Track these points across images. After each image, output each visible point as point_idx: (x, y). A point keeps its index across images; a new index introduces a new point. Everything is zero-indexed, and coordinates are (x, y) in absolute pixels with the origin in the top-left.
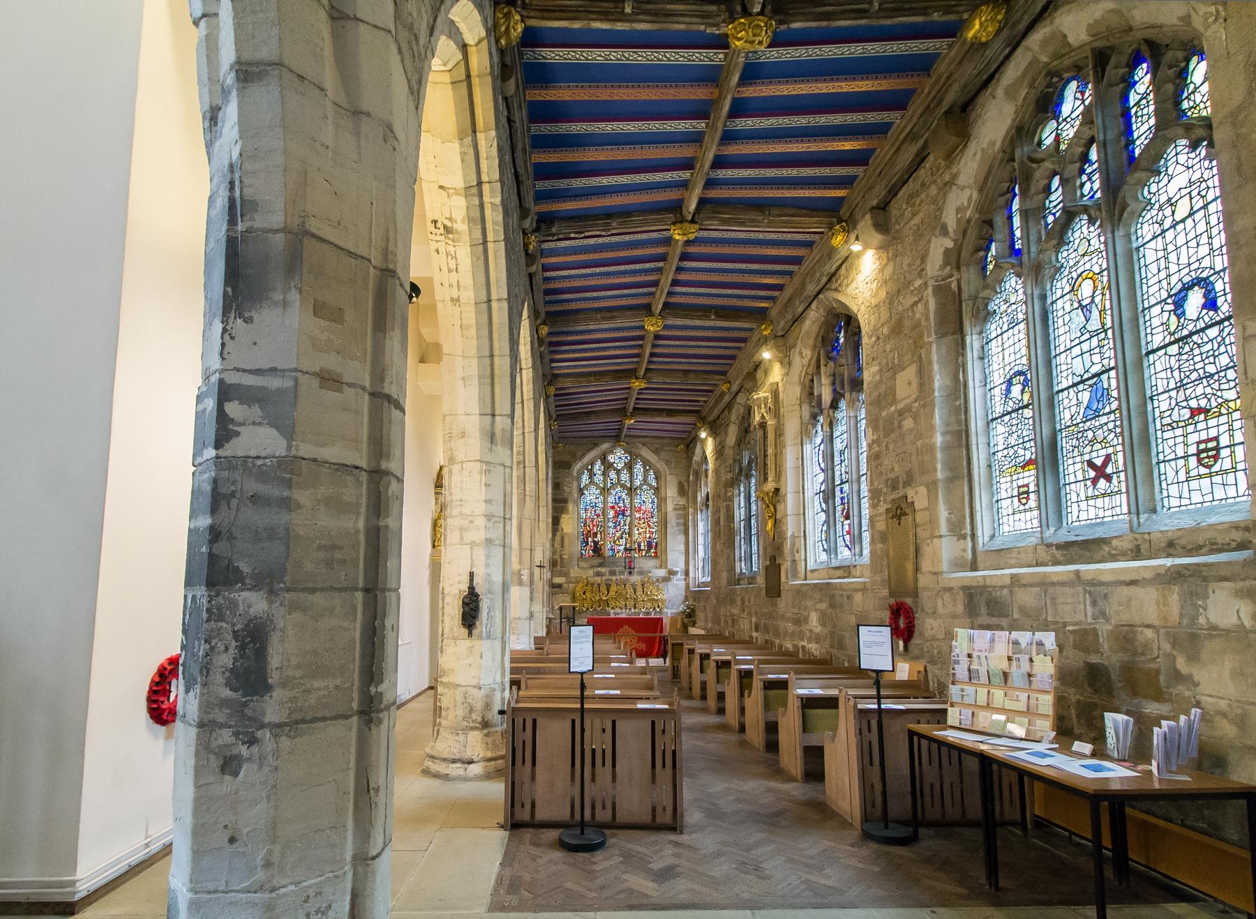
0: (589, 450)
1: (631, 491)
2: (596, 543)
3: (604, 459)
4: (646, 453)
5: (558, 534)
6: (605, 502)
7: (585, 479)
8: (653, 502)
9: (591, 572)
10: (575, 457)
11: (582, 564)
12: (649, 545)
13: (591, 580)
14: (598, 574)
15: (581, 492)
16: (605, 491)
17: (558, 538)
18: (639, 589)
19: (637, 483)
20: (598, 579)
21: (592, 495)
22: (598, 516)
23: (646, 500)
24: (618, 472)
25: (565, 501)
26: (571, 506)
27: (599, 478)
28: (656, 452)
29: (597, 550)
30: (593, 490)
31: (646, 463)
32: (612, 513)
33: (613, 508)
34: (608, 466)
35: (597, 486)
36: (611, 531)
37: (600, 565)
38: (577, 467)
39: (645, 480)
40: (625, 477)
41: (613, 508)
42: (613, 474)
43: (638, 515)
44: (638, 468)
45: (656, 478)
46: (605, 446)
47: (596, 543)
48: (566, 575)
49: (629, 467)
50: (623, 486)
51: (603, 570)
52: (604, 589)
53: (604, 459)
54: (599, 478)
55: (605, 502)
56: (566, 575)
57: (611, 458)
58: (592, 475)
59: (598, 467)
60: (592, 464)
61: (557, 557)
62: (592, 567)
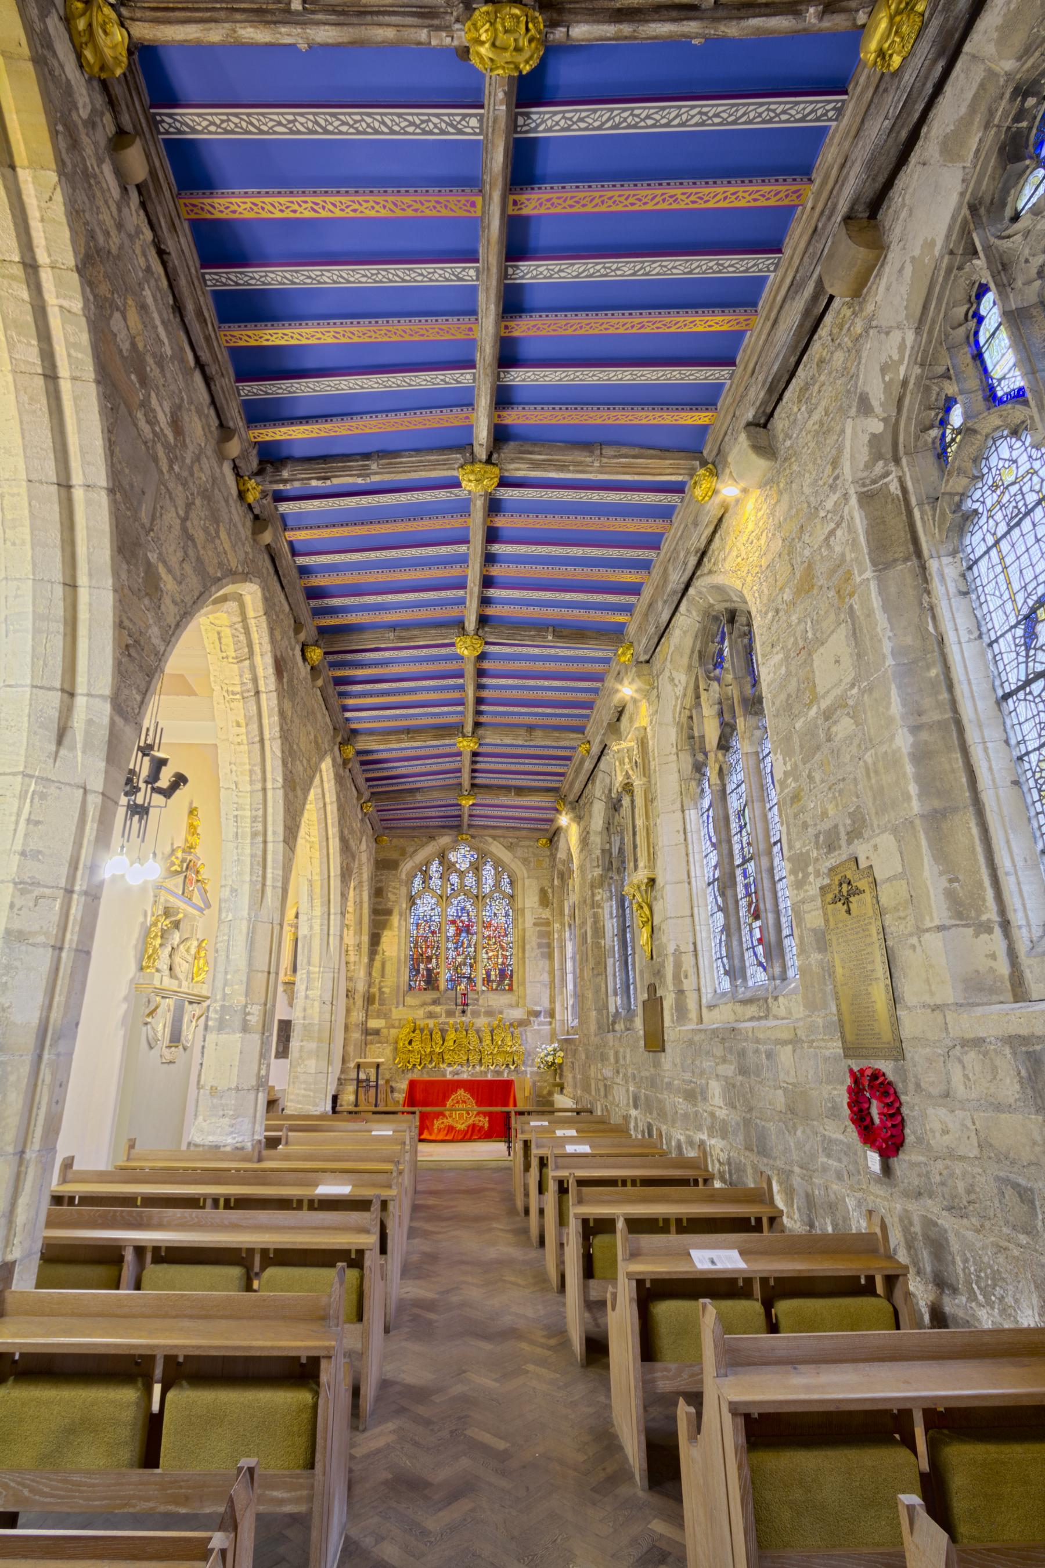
1: (478, 898)
2: (429, 971)
3: (442, 856)
4: (497, 849)
5: (378, 958)
7: (418, 881)
8: (507, 915)
9: (420, 1013)
11: (409, 1000)
12: (502, 973)
13: (421, 1023)
14: (431, 1015)
15: (412, 900)
16: (444, 899)
17: (377, 964)
19: (487, 889)
20: (431, 1023)
21: (426, 905)
22: (433, 933)
24: (461, 874)
25: (389, 912)
28: (510, 847)
32: (452, 931)
33: (453, 922)
37: (435, 1002)
38: (407, 867)
39: (497, 885)
40: (470, 880)
41: (453, 922)
42: (454, 878)
43: (487, 933)
44: (488, 871)
45: (511, 883)
46: (445, 840)
47: (429, 971)
48: (386, 1016)
53: (442, 856)
56: (386, 1016)
57: (452, 857)
58: (426, 878)
59: (435, 866)
60: (428, 864)
61: (374, 990)
62: (424, 1004)
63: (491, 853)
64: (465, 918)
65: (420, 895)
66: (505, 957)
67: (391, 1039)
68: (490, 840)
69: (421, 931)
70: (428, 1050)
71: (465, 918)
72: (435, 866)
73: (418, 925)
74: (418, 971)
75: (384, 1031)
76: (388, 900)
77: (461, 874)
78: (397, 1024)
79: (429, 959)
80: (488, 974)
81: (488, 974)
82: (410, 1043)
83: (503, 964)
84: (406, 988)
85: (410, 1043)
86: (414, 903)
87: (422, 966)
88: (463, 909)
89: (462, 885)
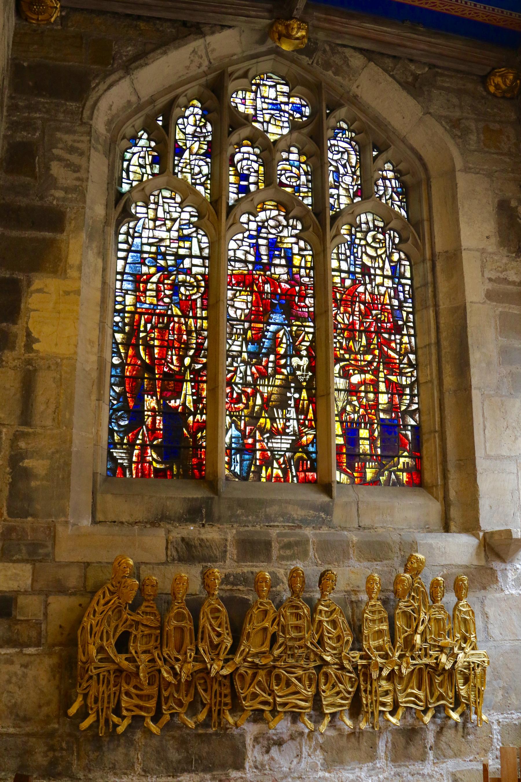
0: (165, 44)
3: (214, 96)
6: (215, 256)
7: (138, 162)
8: (396, 275)
9: (155, 542)
10: (110, 62)
13: (160, 578)
14: (189, 552)
15: (121, 208)
16: (214, 215)
18: (375, 626)
19: (341, 198)
20: (190, 575)
21: (161, 224)
22: (187, 306)
23: (368, 259)
24: (268, 152)
26: (77, 248)
27: (193, 166)
28: (414, 87)
29: (181, 449)
30: (168, 205)
31: (373, 141)
32: (240, 304)
33: (245, 282)
34: (227, 126)
35: (187, 194)
36: (243, 371)
37: (195, 513)
38: (114, 97)
40: (292, 168)
41: (245, 282)
43: (343, 319)
45: (405, 192)
46: (225, 43)
47: (174, 418)
49: (312, 138)
50: (287, 205)
51: (211, 534)
52: (216, 627)
53: (214, 96)
54: (193, 166)
55: (215, 256)
57: (243, 102)
58: (166, 153)
59: (190, 123)
60: (170, 111)
62: (159, 519)
63: (354, 100)
64: (280, 272)
65: (144, 193)
66: (394, 389)
67: (51, 629)
68: (357, 60)
69: (150, 299)
70: (186, 671)
71: (280, 272)
72: (190, 123)
73: (138, 279)
74: (136, 416)
75: (30, 606)
76: (53, 182)
77: (268, 152)
78: (73, 578)
79: (173, 383)
80: (351, 435)
81: (351, 435)
82: (122, 644)
83: (392, 407)
84: (102, 466)
85: (122, 644)
86: (126, 215)
87: (150, 402)
88: (273, 245)
89: (269, 178)
